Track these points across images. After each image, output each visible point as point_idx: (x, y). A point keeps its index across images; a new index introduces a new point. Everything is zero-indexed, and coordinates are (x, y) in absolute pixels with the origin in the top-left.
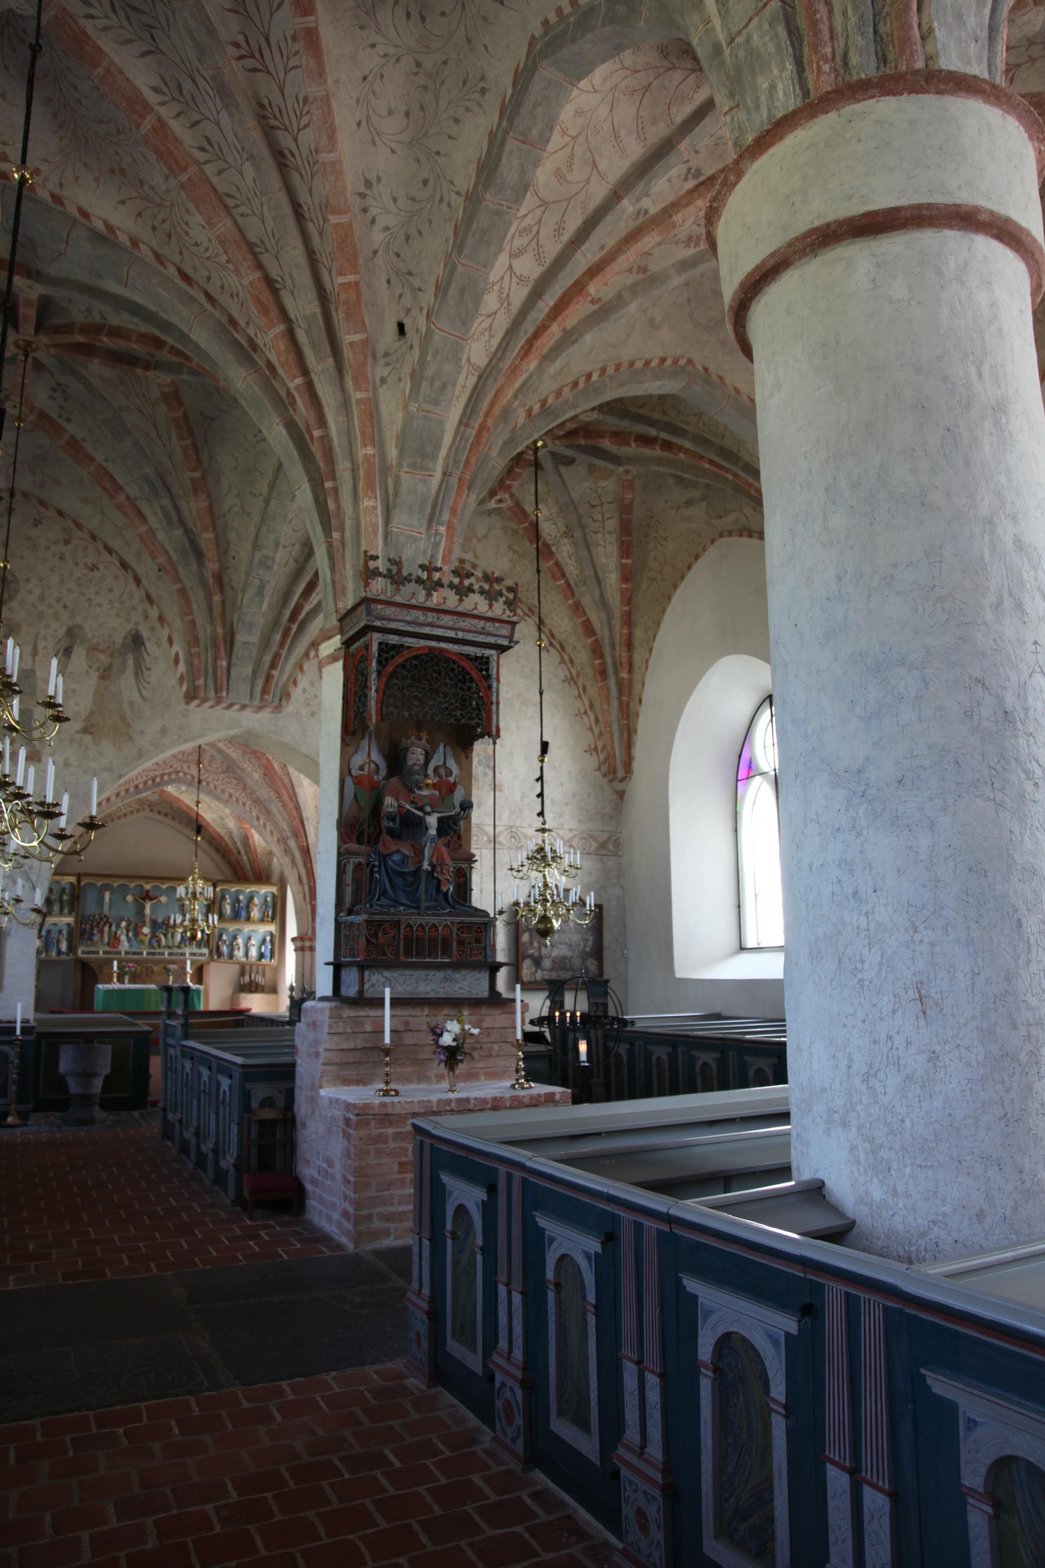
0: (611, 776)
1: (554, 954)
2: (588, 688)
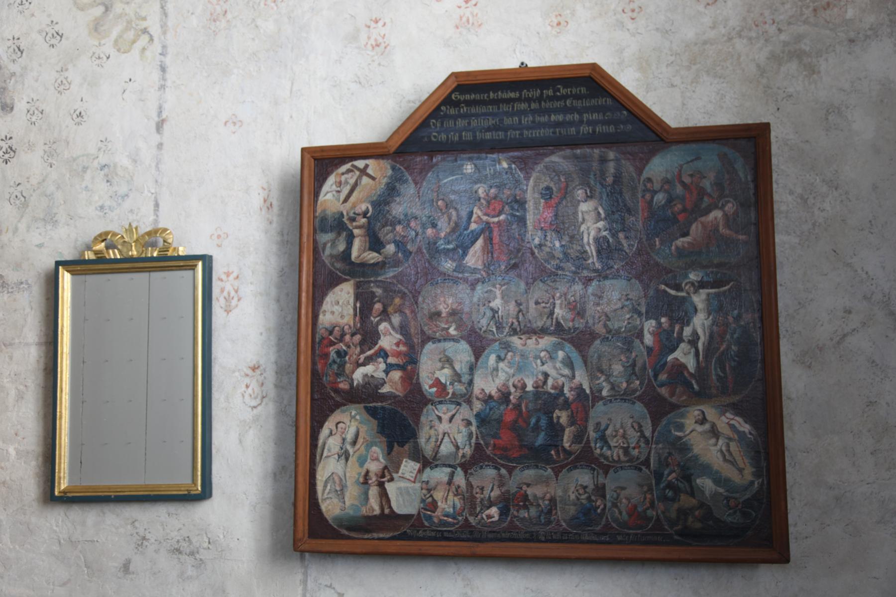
1: (487, 384)
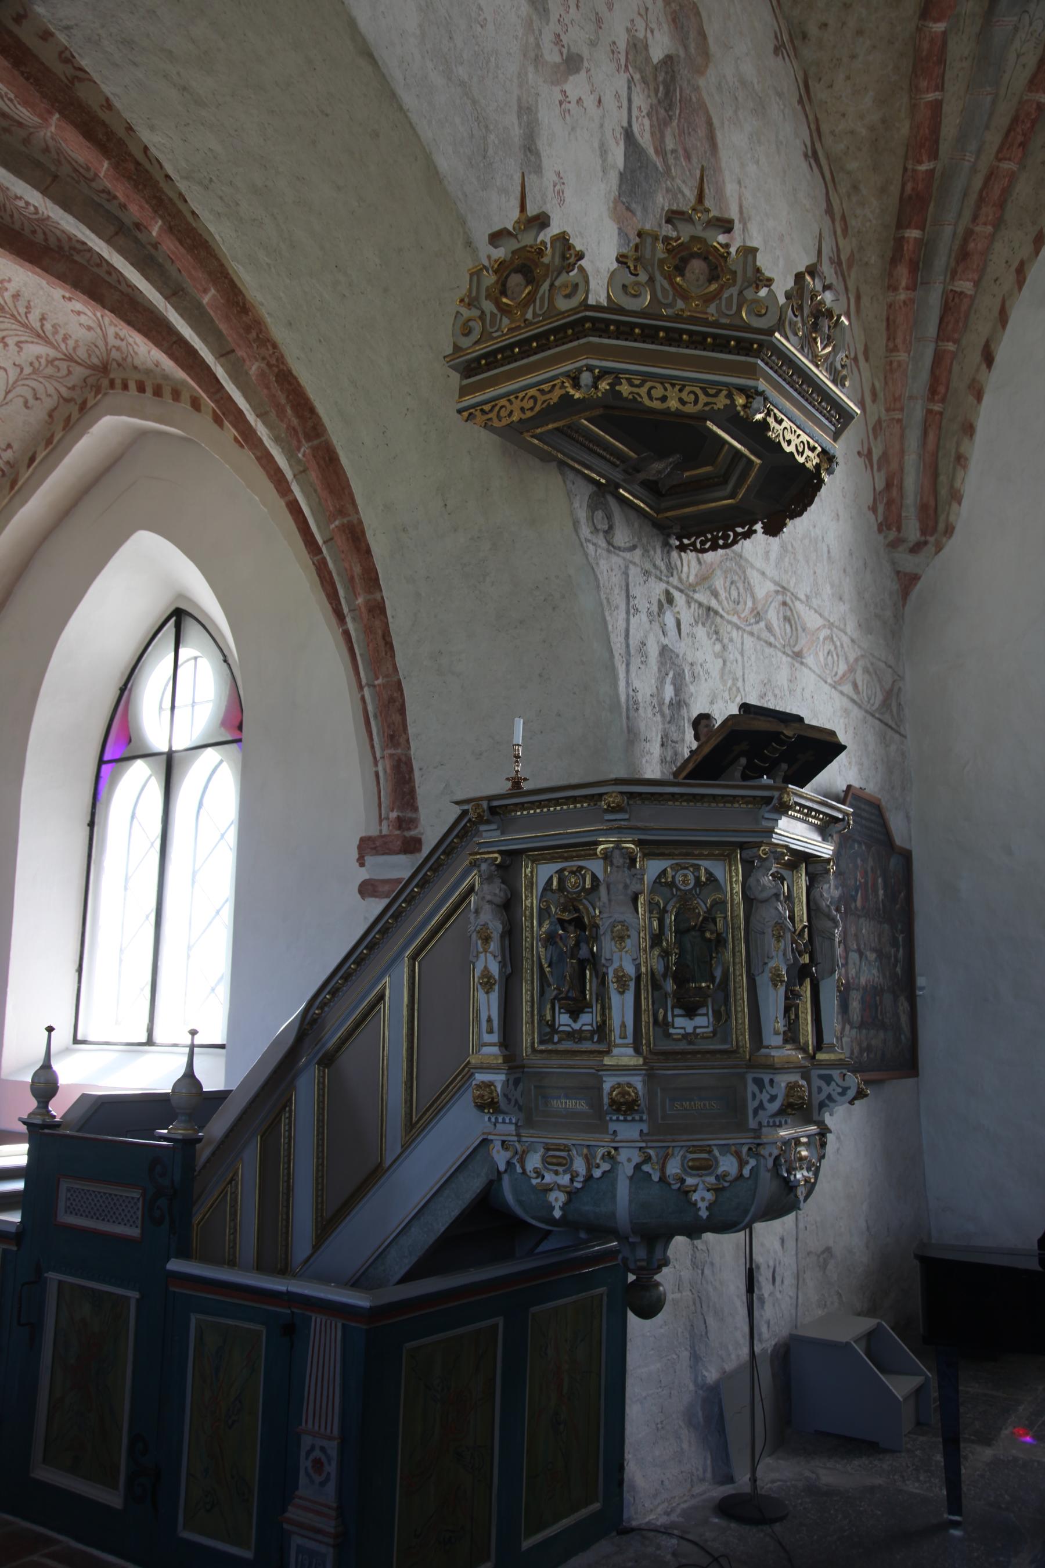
0: (893, 534)
1: (863, 981)
2: (865, 301)
